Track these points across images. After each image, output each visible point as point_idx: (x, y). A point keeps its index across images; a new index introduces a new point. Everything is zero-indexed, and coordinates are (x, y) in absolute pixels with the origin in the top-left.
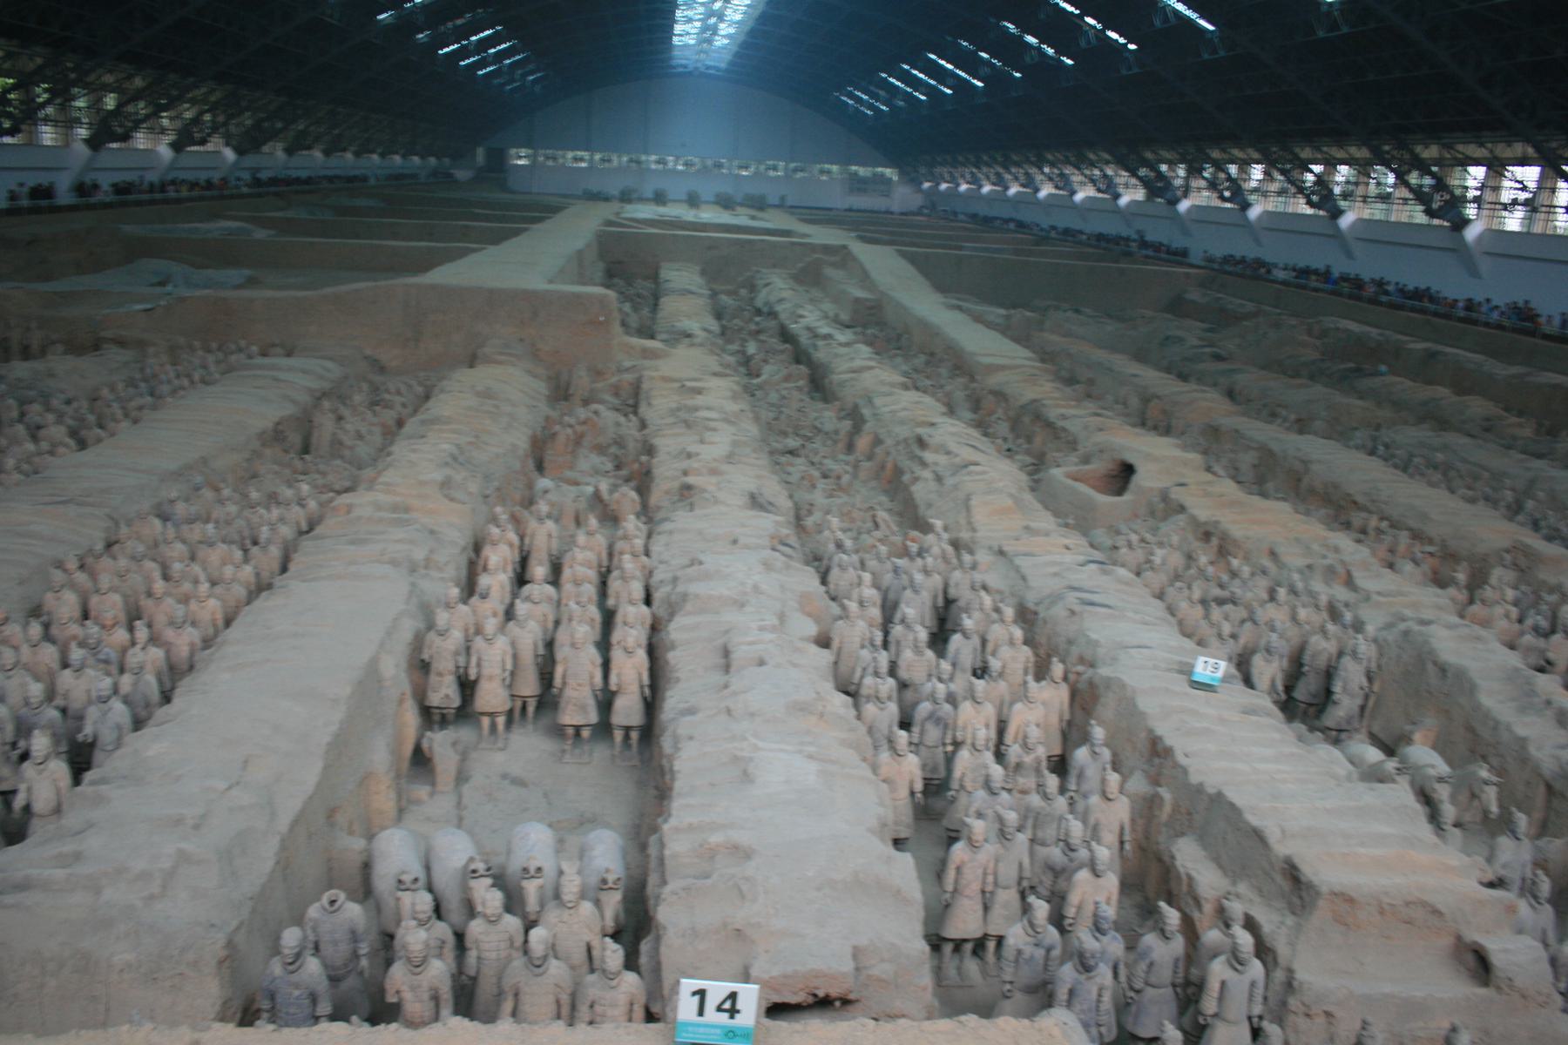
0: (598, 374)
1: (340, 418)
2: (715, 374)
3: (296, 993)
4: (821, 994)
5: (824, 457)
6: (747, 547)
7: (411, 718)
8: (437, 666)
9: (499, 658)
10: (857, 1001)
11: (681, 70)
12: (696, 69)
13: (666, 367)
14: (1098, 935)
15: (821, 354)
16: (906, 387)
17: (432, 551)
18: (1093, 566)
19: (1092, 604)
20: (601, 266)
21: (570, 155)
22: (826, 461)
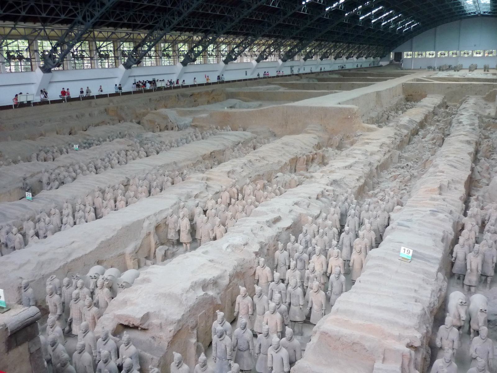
0: (348, 137)
2: (388, 138)
3: (25, 297)
4: (131, 323)
5: (413, 170)
6: (301, 197)
7: (153, 240)
8: (170, 226)
9: (185, 225)
10: (147, 329)
11: (472, 14)
12: (479, 13)
13: (372, 135)
15: (452, 130)
16: (469, 142)
17: (201, 193)
18: (429, 212)
19: (402, 225)
20: (402, 96)
21: (428, 53)
22: (412, 171)
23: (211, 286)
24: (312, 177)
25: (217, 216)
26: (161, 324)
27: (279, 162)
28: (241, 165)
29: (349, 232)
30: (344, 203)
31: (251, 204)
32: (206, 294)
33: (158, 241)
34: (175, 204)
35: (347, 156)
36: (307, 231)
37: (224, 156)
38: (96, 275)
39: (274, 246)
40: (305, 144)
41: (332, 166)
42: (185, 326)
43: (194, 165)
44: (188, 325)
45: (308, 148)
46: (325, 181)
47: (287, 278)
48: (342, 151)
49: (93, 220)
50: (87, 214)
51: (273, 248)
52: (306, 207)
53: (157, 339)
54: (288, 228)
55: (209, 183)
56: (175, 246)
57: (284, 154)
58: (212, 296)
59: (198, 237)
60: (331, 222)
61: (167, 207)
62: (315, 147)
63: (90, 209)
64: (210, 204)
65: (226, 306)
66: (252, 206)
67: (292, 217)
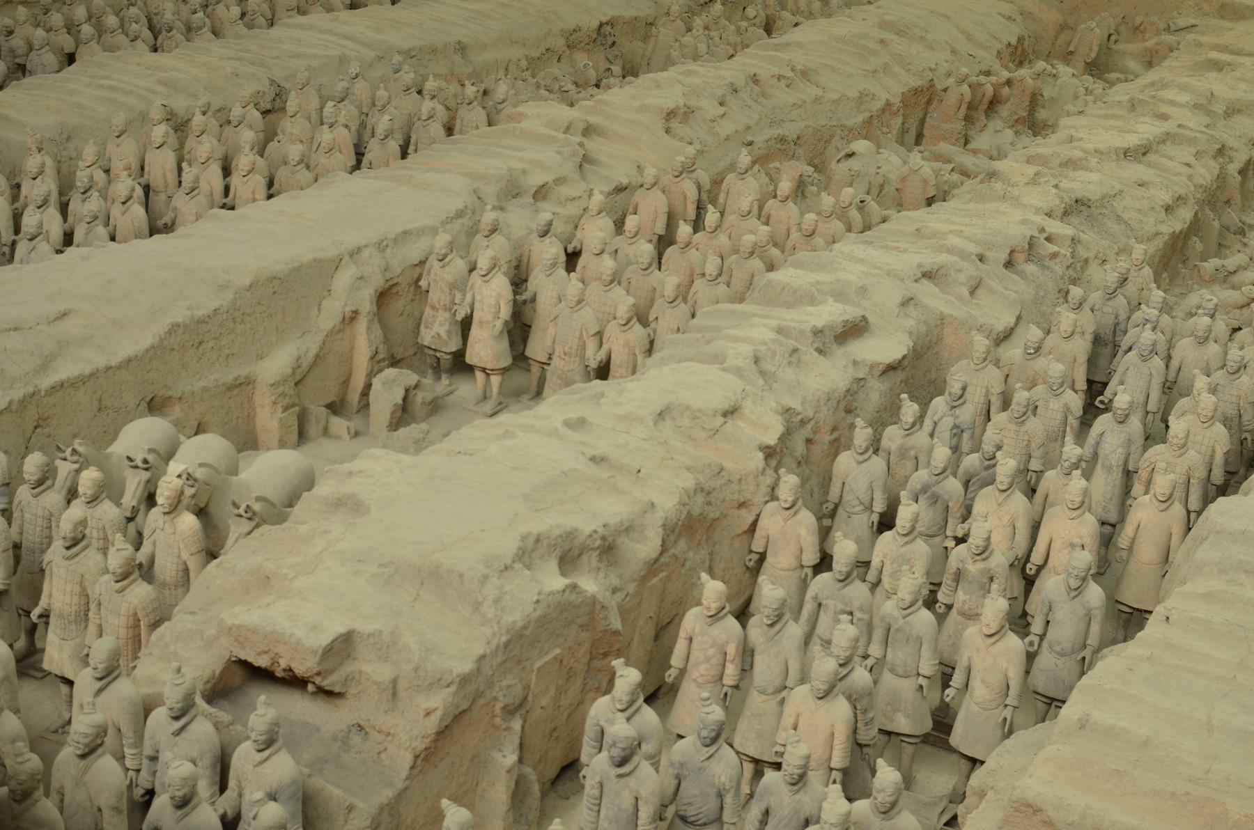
0: (1137, 29)
1: (689, 30)
4: (283, 663)
6: (950, 251)
7: (363, 343)
8: (434, 296)
9: (493, 301)
10: (340, 695)
14: (699, 744)
17: (560, 181)
23: (591, 559)
24: (992, 175)
25: (619, 283)
26: (395, 682)
27: (864, 97)
28: (719, 92)
29: (1127, 416)
30: (1112, 295)
31: (752, 253)
32: (574, 587)
33: (381, 347)
34: (460, 214)
35: (1133, 106)
36: (964, 389)
37: (651, 45)
38: (150, 458)
39: (834, 429)
40: (969, 37)
41: (1071, 139)
42: (482, 701)
43: (533, 65)
44: (495, 699)
45: (980, 53)
46: (1043, 196)
47: (875, 563)
48: (1112, 84)
49: (138, 236)
50: (116, 211)
51: (828, 438)
52: (965, 292)
53: (373, 733)
54: (891, 368)
55: (595, 145)
56: (444, 376)
57: (886, 68)
58: (594, 598)
59: (536, 349)
60: (1060, 367)
61: (428, 222)
62: (1006, 54)
63: (133, 190)
64: (595, 232)
65: (636, 639)
66: (756, 263)
67: (910, 323)
